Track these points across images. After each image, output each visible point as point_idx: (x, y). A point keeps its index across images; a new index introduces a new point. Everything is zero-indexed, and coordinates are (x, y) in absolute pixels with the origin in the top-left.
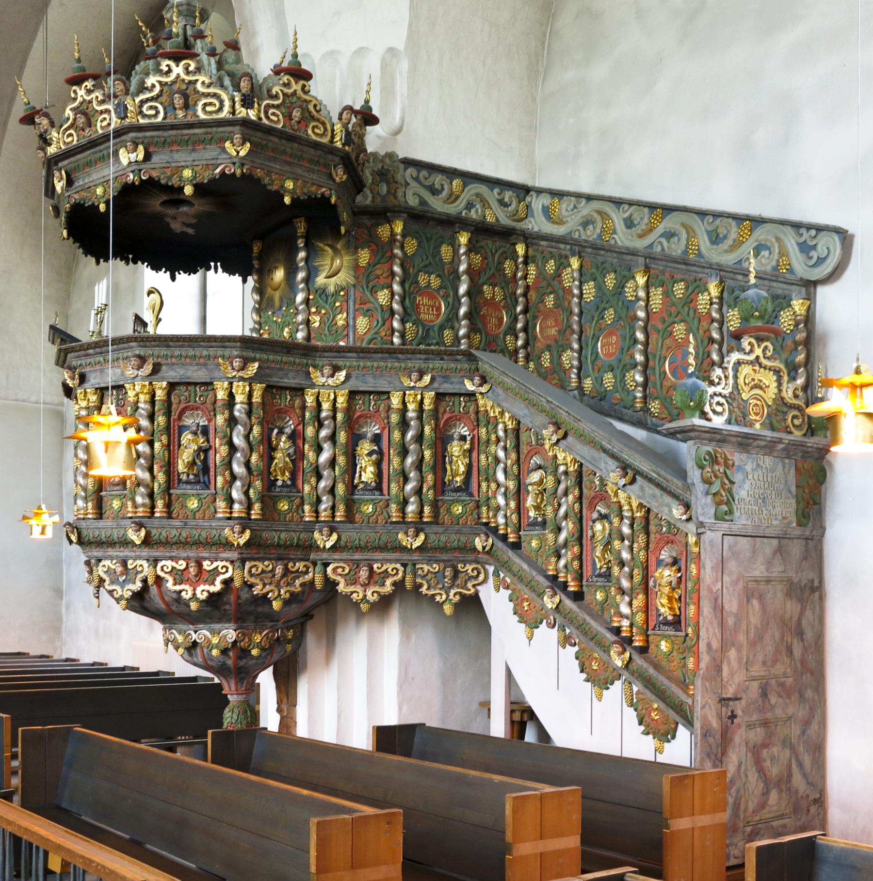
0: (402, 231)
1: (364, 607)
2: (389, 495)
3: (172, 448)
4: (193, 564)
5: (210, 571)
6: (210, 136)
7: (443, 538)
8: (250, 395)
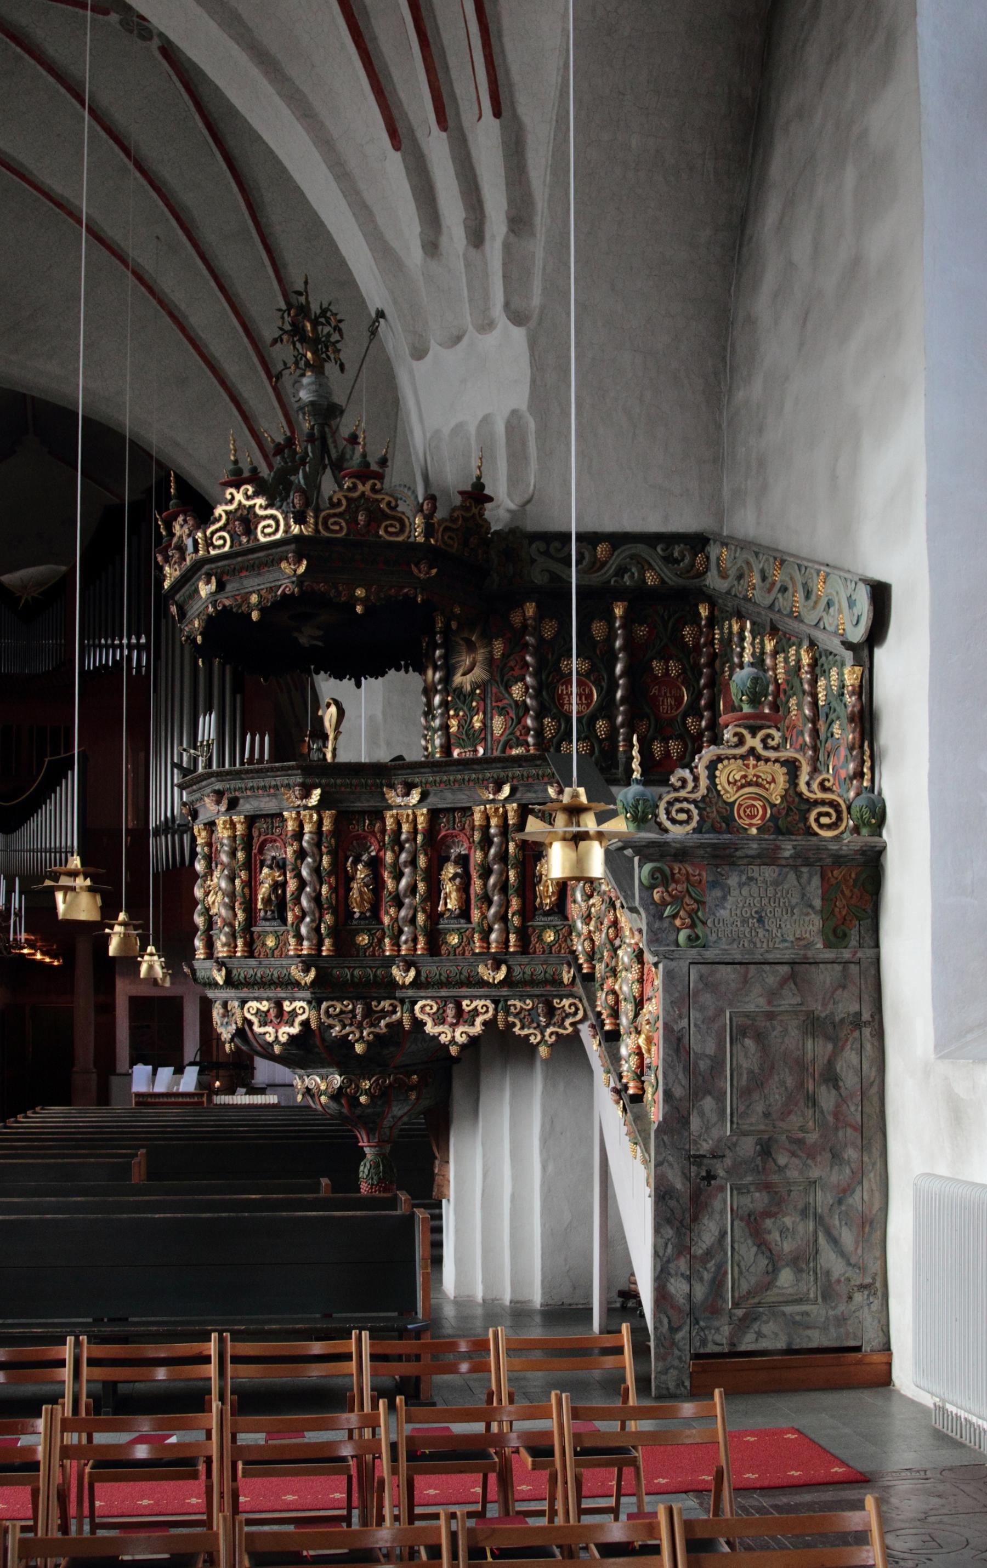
0: (535, 613)
3: (251, 885)
8: (320, 822)
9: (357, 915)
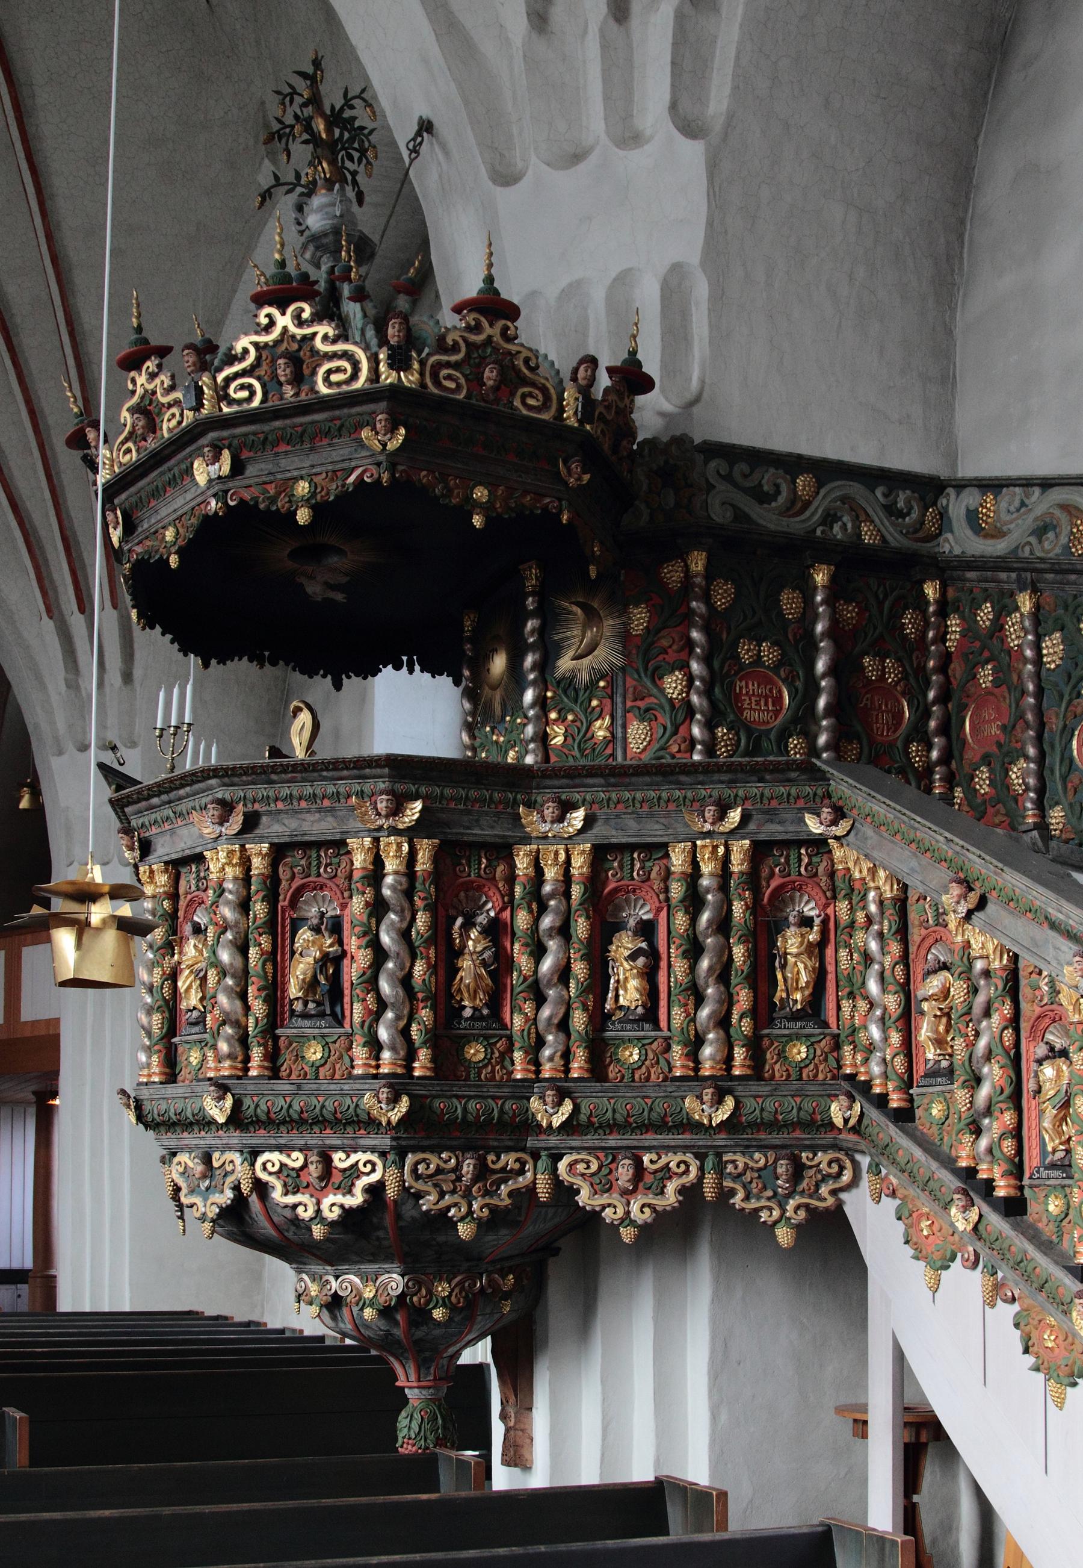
1: (627, 1234)
2: (669, 1030)
4: (314, 1158)
5: (344, 1170)
6: (338, 423)
7: (770, 1105)
9: (468, 1013)
